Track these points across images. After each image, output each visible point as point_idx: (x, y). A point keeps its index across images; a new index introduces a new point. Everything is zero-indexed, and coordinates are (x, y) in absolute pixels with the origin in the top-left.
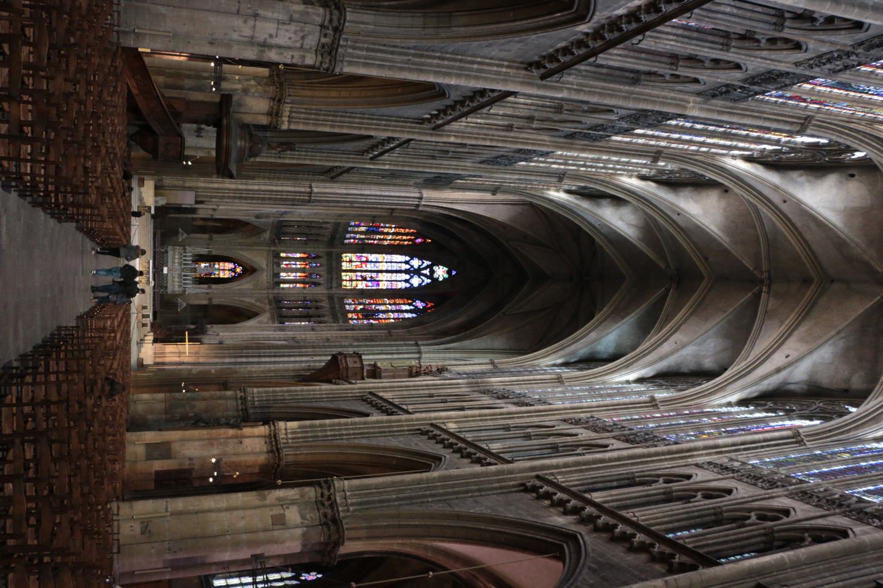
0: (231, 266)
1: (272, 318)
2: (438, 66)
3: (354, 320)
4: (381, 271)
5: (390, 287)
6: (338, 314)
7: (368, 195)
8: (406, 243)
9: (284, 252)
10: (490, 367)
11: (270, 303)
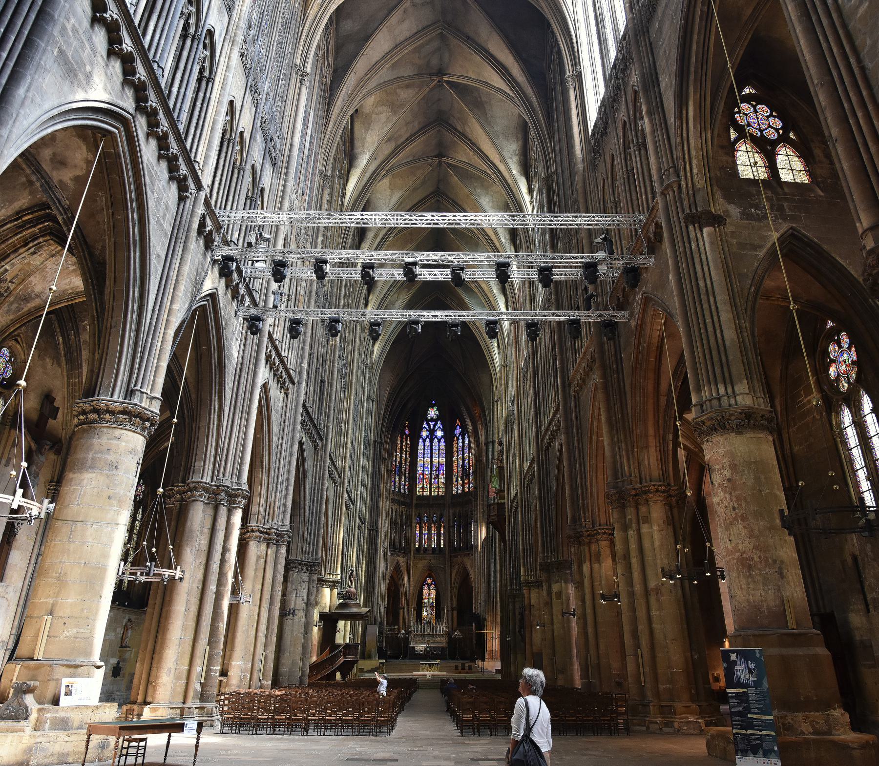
0: (426, 588)
1: (468, 555)
2: (317, 503)
3: (469, 487)
4: (431, 462)
5: (444, 455)
6: (466, 499)
7: (373, 484)
8: (408, 442)
9: (415, 545)
10: (499, 403)
11: (455, 557)
